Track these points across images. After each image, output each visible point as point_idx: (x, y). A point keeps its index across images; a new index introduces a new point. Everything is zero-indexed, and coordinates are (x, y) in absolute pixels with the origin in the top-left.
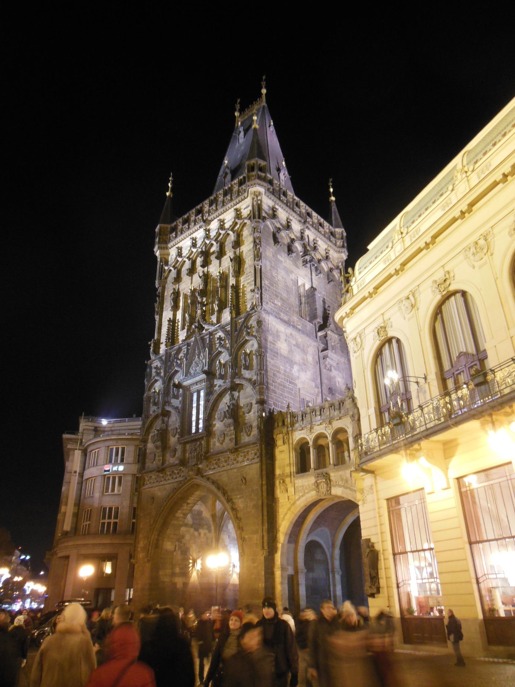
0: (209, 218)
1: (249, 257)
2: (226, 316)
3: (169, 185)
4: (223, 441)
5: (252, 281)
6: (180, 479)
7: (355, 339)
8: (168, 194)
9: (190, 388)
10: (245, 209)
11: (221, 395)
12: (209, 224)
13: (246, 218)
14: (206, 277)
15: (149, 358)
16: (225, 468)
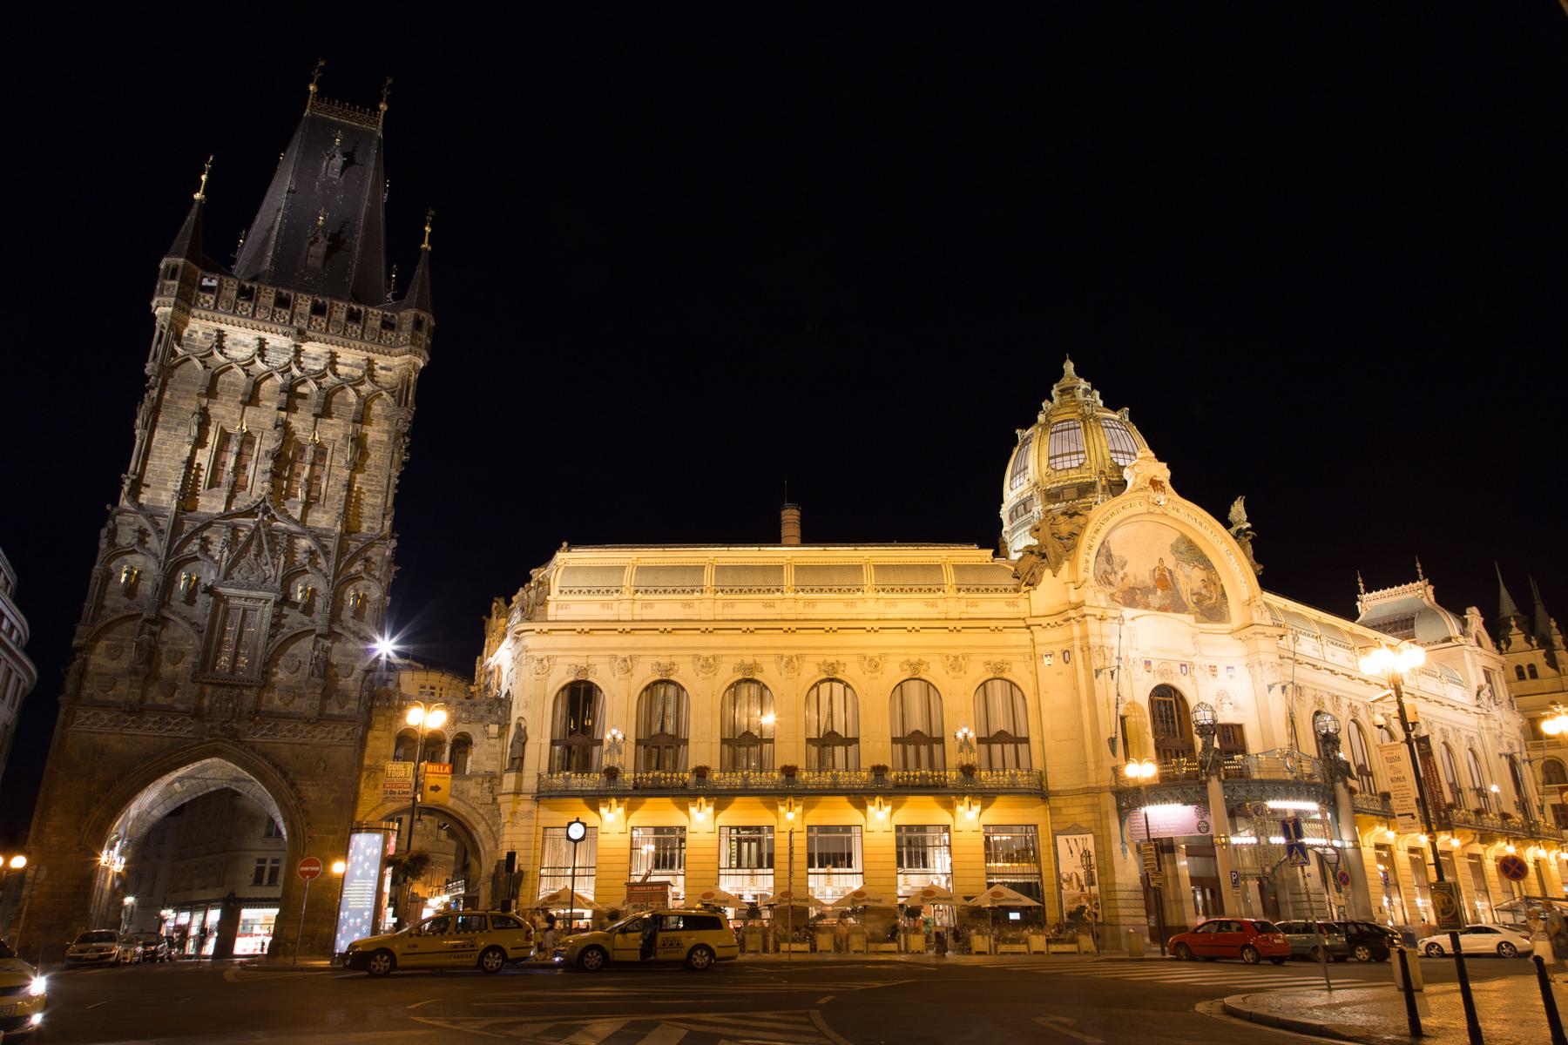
0: (309, 334)
1: (376, 451)
2: (323, 519)
3: (204, 178)
4: (292, 701)
5: (379, 492)
6: (182, 734)
7: (542, 660)
8: (197, 196)
9: (228, 599)
10: (382, 368)
11: (297, 637)
12: (303, 342)
13: (386, 389)
14: (285, 428)
15: (115, 503)
16: (287, 740)
